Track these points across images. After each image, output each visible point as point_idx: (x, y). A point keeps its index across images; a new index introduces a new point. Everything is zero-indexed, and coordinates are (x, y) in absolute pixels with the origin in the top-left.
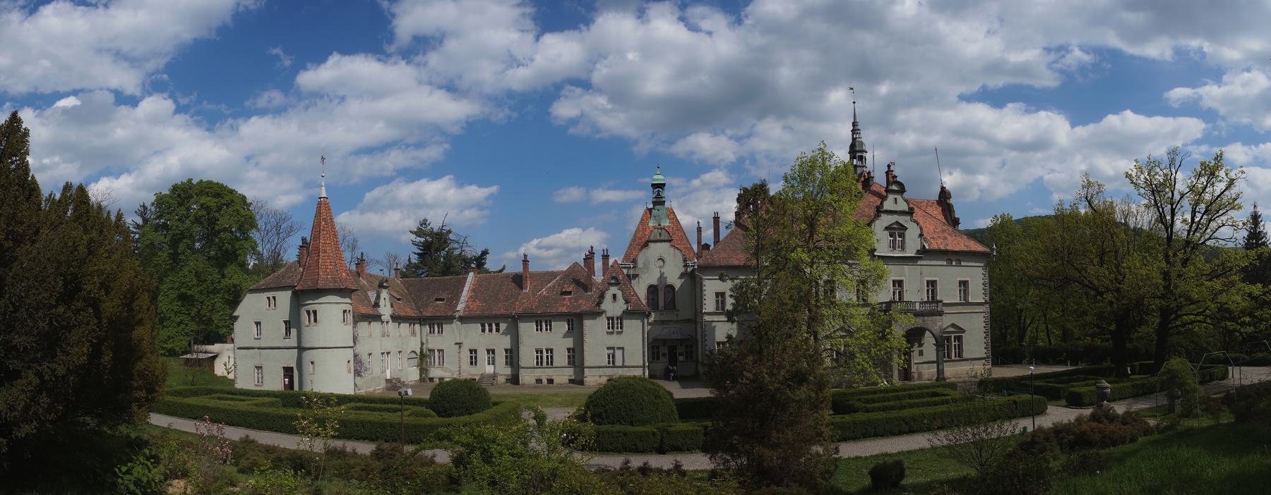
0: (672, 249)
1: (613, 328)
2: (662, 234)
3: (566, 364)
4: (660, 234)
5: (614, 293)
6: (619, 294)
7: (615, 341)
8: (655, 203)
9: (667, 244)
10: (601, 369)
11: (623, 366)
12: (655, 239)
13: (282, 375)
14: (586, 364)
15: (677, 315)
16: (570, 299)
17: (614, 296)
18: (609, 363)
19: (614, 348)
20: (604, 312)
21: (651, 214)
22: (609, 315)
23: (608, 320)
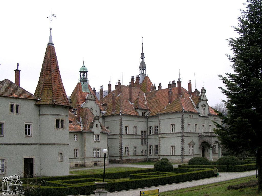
0: (96, 105)
2: (92, 97)
3: (74, 157)
7: (97, 146)
9: (93, 102)
10: (92, 159)
13: (24, 164)
17: (97, 125)
22: (95, 133)
23: (94, 135)
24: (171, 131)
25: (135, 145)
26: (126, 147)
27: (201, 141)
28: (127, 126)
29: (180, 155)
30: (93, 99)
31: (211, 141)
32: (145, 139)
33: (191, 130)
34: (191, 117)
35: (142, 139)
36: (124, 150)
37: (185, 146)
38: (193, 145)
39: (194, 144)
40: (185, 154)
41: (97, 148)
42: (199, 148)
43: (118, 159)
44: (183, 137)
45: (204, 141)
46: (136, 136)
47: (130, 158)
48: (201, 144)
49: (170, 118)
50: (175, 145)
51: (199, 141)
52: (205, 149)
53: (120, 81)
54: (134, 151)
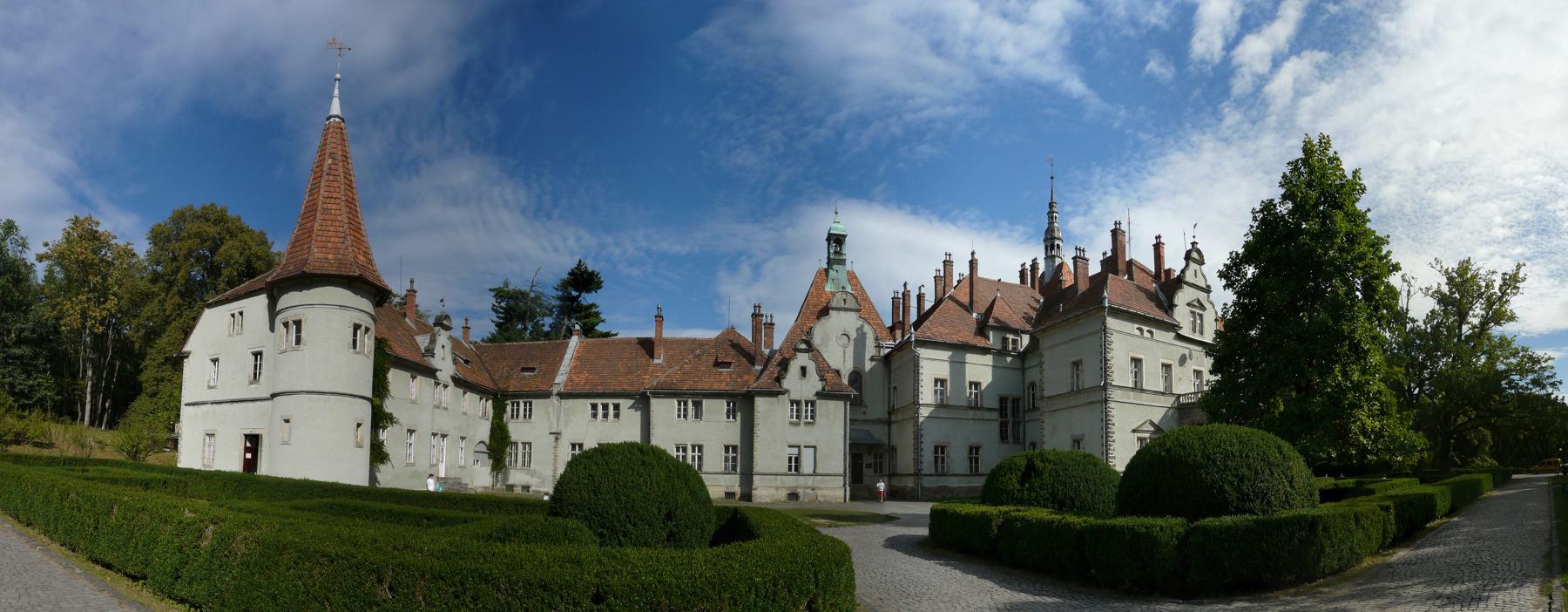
1: (798, 417)
4: (845, 300)
5: (804, 364)
6: (811, 367)
7: (802, 435)
8: (830, 262)
10: (778, 477)
11: (815, 474)
12: (838, 306)
14: (757, 469)
15: (864, 413)
16: (730, 374)
17: (804, 369)
18: (790, 469)
19: (799, 447)
20: (787, 391)
21: (827, 275)
22: (794, 396)
23: (792, 405)
24: (1073, 385)
25: (974, 440)
26: (936, 448)
28: (941, 377)
30: (853, 307)
32: (1016, 424)
35: (1003, 426)
36: (928, 456)
41: (804, 444)
43: (910, 483)
46: (978, 412)
47: (953, 483)
49: (1071, 340)
50: (1083, 435)
53: (950, 255)
54: (971, 463)
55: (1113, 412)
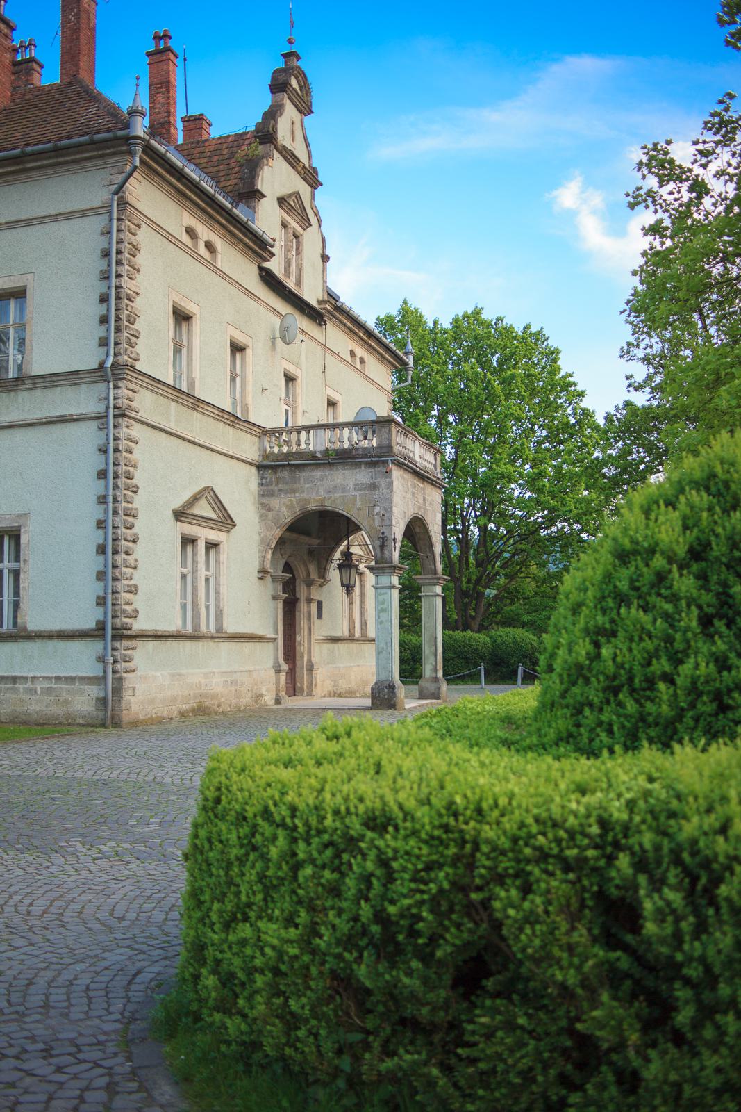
27: (286, 508)
29: (91, 625)
31: (389, 510)
33: (197, 374)
34: (202, 250)
37: (140, 526)
38: (213, 536)
39: (227, 522)
40: (138, 625)
42: (263, 572)
44: (123, 422)
45: (313, 506)
48: (281, 542)
50: (26, 516)
51: (264, 508)
52: (302, 592)
55: (138, 455)
